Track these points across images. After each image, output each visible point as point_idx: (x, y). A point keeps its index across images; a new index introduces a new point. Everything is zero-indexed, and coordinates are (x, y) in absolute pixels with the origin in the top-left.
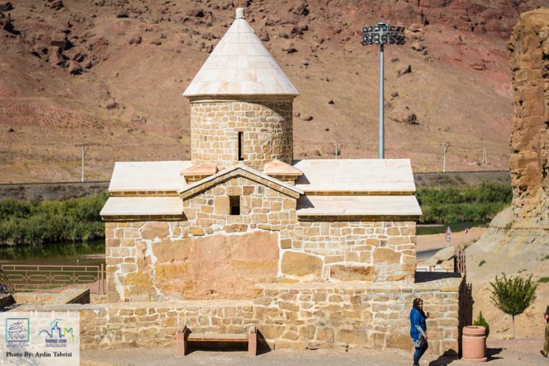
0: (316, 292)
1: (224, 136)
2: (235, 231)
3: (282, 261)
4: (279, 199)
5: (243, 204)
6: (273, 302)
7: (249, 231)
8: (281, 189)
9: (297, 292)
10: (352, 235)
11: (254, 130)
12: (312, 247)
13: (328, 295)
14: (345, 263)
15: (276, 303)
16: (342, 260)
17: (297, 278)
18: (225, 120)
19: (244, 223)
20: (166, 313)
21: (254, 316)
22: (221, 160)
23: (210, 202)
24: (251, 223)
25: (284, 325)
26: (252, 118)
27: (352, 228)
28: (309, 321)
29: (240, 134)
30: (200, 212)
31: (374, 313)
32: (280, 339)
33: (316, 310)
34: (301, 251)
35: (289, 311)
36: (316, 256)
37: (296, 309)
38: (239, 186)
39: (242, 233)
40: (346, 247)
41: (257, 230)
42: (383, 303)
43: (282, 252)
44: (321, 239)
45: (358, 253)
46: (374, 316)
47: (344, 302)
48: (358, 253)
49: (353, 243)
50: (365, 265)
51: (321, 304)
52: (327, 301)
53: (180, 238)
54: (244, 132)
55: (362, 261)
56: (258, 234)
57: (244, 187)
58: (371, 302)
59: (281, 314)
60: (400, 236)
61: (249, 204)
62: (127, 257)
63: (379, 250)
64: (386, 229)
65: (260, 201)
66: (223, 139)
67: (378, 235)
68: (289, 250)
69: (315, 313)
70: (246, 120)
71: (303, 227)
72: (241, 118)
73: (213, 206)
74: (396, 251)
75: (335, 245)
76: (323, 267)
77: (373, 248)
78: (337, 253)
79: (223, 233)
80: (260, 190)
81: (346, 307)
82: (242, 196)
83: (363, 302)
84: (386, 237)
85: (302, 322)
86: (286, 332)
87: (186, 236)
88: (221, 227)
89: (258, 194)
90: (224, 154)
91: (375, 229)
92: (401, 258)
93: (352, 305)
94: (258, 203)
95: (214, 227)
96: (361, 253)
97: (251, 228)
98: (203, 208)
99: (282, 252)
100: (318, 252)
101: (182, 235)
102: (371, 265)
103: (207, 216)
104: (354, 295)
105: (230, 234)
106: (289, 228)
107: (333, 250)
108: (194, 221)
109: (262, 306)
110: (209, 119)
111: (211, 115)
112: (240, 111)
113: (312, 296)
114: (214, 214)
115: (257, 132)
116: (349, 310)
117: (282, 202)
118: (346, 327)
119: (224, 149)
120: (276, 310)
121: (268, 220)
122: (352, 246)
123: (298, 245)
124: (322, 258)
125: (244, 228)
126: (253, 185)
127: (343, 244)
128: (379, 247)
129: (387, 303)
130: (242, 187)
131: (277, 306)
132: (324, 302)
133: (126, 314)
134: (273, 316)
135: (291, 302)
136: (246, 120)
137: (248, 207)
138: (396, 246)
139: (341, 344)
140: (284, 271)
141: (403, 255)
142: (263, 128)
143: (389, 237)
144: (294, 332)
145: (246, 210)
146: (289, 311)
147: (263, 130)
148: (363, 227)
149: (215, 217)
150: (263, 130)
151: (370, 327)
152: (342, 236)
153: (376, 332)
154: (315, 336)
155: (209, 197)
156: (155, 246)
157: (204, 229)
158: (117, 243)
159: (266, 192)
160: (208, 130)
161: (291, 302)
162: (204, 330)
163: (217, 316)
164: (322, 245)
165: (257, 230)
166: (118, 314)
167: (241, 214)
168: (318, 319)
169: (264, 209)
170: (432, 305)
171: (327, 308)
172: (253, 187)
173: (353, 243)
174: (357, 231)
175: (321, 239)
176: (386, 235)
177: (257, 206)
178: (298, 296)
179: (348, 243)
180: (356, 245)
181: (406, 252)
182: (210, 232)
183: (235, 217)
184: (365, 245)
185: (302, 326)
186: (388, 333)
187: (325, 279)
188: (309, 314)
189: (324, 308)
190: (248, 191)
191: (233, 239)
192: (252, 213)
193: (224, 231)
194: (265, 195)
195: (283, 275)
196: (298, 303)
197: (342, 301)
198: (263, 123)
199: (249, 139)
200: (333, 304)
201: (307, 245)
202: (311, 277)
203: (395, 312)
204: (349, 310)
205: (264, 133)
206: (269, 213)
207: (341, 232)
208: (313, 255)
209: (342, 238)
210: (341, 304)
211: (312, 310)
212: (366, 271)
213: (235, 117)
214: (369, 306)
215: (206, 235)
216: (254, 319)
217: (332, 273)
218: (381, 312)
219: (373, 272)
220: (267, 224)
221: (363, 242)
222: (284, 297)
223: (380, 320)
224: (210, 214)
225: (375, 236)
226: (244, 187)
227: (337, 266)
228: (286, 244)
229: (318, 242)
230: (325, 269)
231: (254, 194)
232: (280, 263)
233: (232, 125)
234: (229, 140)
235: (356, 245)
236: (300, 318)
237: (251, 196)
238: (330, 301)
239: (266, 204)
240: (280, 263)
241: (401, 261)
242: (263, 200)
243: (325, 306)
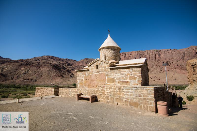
4: (106, 65)
5: (99, 67)
7: (100, 73)
8: (106, 62)
9: (105, 86)
10: (123, 72)
12: (113, 76)
13: (112, 88)
14: (121, 80)
16: (120, 79)
17: (110, 84)
21: (95, 92)
23: (93, 67)
25: (102, 95)
27: (123, 71)
28: (108, 95)
29: (105, 55)
31: (125, 94)
32: (101, 99)
33: (109, 92)
34: (111, 77)
35: (103, 91)
37: (105, 91)
39: (99, 73)
40: (121, 76)
41: (101, 72)
42: (127, 91)
43: (107, 77)
44: (115, 74)
46: (125, 95)
47: (117, 90)
48: (125, 77)
49: (123, 75)
50: (127, 80)
52: (112, 89)
53: (88, 75)
56: (102, 73)
58: (124, 90)
59: (101, 92)
63: (130, 76)
64: (132, 70)
65: (102, 65)
67: (130, 72)
69: (109, 93)
71: (111, 71)
74: (135, 76)
75: (119, 75)
77: (129, 76)
79: (95, 73)
80: (102, 63)
85: (106, 95)
86: (102, 97)
87: (89, 74)
88: (95, 72)
91: (129, 71)
92: (137, 79)
93: (118, 91)
94: (101, 66)
95: (94, 72)
99: (107, 77)
102: (128, 80)
103: (92, 70)
104: (119, 88)
105: (96, 74)
106: (108, 71)
107: (118, 77)
109: (97, 90)
116: (118, 92)
118: (117, 97)
120: (100, 91)
122: (123, 76)
123: (110, 76)
124: (116, 79)
125: (99, 72)
127: (121, 75)
131: (100, 90)
132: (111, 90)
134: (99, 92)
135: (103, 89)
138: (135, 75)
139: (116, 102)
140: (107, 82)
143: (133, 73)
144: (104, 97)
146: (103, 91)
149: (93, 70)
151: (124, 98)
153: (126, 100)
154: (109, 99)
156: (84, 76)
158: (78, 76)
161: (103, 89)
162: (86, 95)
164: (115, 75)
165: (101, 72)
168: (110, 94)
170: (144, 92)
171: (112, 91)
173: (123, 75)
174: (124, 71)
175: (115, 74)
176: (132, 72)
178: (105, 87)
181: (138, 77)
184: (126, 75)
186: (129, 101)
188: (108, 93)
190: (100, 64)
191: (97, 75)
196: (105, 89)
197: (116, 89)
200: (114, 90)
201: (112, 76)
202: (113, 84)
203: (131, 94)
204: (118, 92)
211: (108, 92)
212: (127, 82)
214: (123, 91)
216: (95, 93)
217: (118, 83)
218: (127, 94)
221: (126, 74)
222: (102, 88)
223: (127, 96)
227: (119, 81)
228: (107, 75)
229: (114, 75)
230: (116, 81)
232: (106, 80)
233: (104, 53)
235: (124, 75)
236: (105, 94)
237: (100, 65)
238: (113, 89)
239: (103, 66)
240: (106, 80)
241: (137, 80)
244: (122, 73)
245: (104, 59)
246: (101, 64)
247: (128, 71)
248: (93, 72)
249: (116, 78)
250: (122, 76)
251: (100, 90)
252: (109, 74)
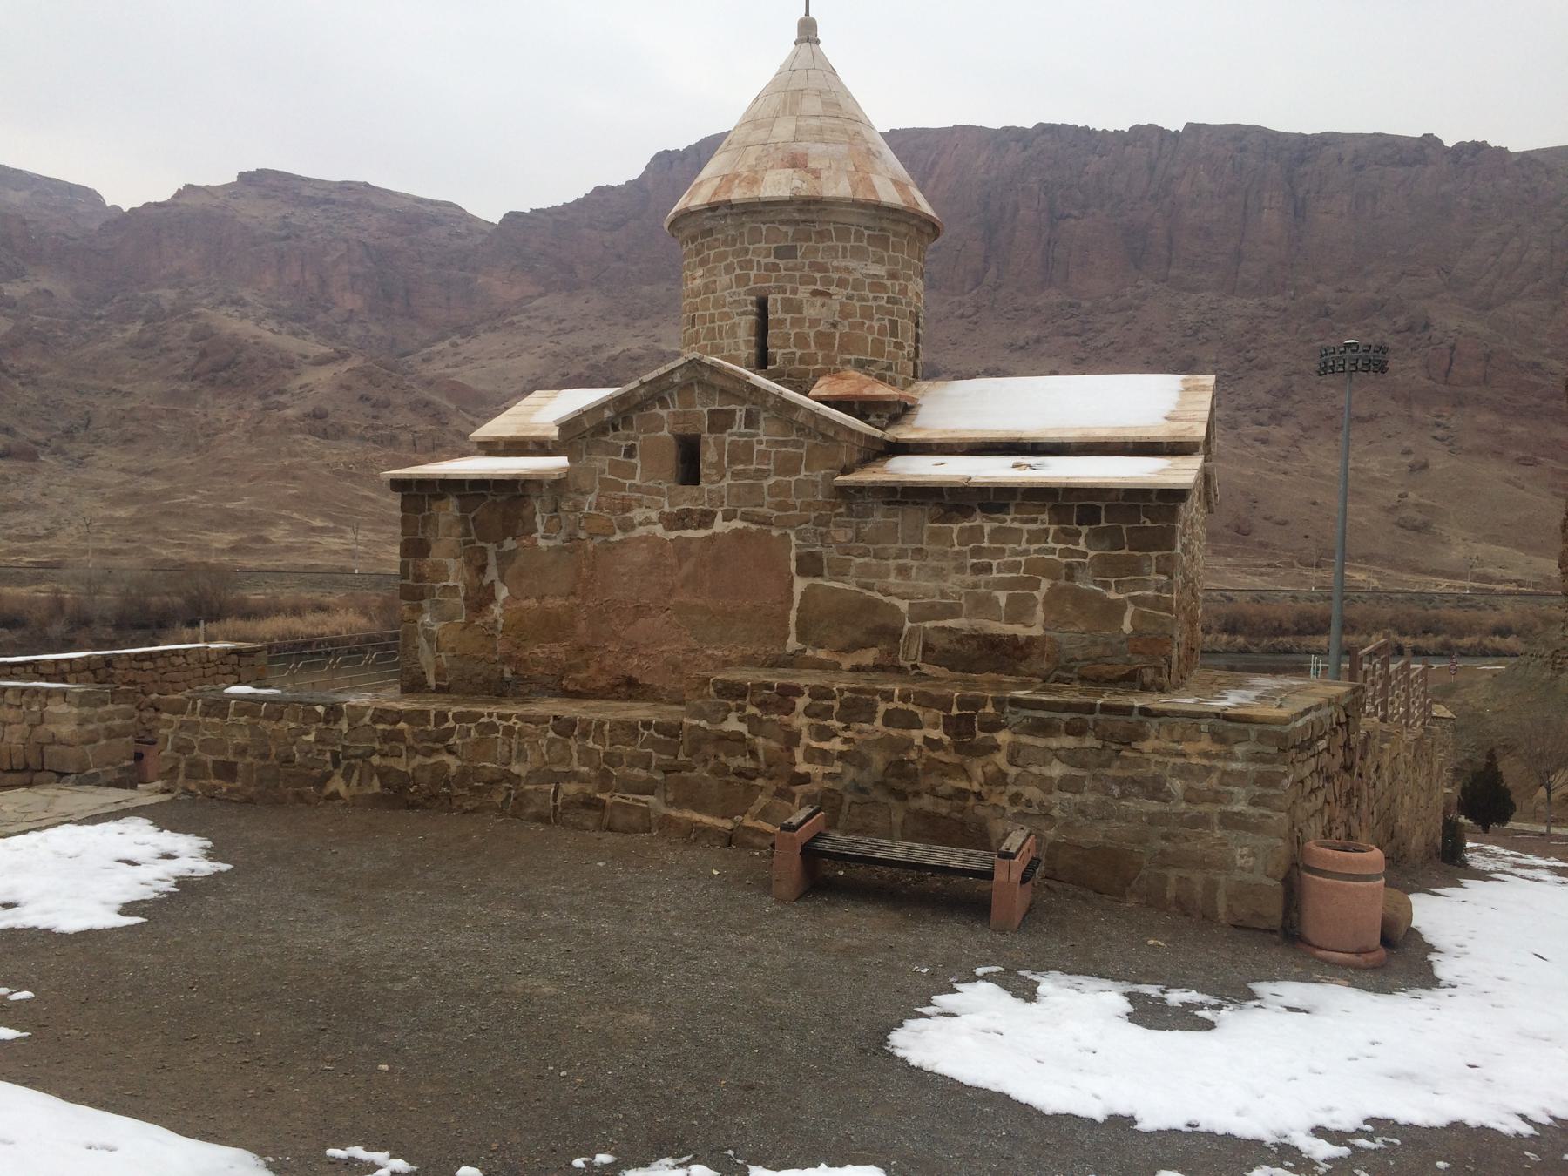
0: (847, 694)
1: (726, 309)
2: (685, 527)
3: (799, 610)
5: (709, 455)
6: (733, 717)
7: (720, 526)
9: (798, 692)
10: (986, 544)
11: (794, 291)
13: (882, 707)
15: (741, 720)
18: (729, 269)
19: (706, 507)
20: (472, 725)
24: (726, 507)
25: (760, 782)
26: (791, 262)
27: (988, 527)
29: (763, 306)
32: (748, 822)
33: (845, 748)
36: (886, 599)
38: (699, 408)
39: (701, 533)
40: (969, 578)
41: (738, 524)
43: (800, 585)
45: (1002, 597)
48: (1002, 597)
50: (1019, 630)
51: (860, 732)
52: (878, 723)
54: (770, 297)
55: (1011, 620)
57: (710, 412)
58: (1003, 737)
60: (1124, 552)
61: (721, 456)
63: (1062, 590)
68: (818, 581)
69: (842, 756)
70: (775, 267)
72: (764, 261)
73: (636, 461)
77: (1045, 584)
78: (943, 594)
79: (659, 530)
80: (751, 420)
81: (931, 743)
82: (706, 435)
83: (980, 735)
84: (1085, 555)
85: (805, 778)
87: (571, 538)
88: (654, 515)
89: (743, 430)
91: (1053, 528)
93: (947, 739)
94: (741, 453)
95: (638, 514)
96: (1010, 599)
97: (725, 519)
98: (614, 466)
99: (800, 585)
100: (892, 590)
101: (562, 535)
102: (1037, 631)
103: (622, 487)
104: (955, 711)
105: (673, 535)
108: (591, 498)
109: (703, 723)
110: (700, 272)
111: (703, 263)
112: (763, 244)
113: (836, 705)
114: (637, 481)
115: (800, 296)
117: (803, 451)
119: (726, 342)
120: (738, 738)
121: (767, 498)
122: (983, 577)
123: (840, 572)
124: (904, 605)
125: (706, 519)
126: (732, 407)
127: (960, 569)
128: (1062, 583)
129: (1054, 743)
131: (743, 728)
132: (866, 726)
133: (385, 721)
134: (731, 753)
136: (775, 267)
137: (718, 465)
140: (802, 637)
141: (1131, 609)
142: (819, 287)
143: (1092, 553)
145: (714, 471)
147: (815, 293)
148: (1016, 525)
149: (637, 489)
150: (815, 293)
152: (957, 548)
155: (628, 438)
157: (613, 518)
159: (762, 422)
163: (590, 744)
164: (903, 571)
165: (738, 524)
166: (367, 720)
167: (702, 484)
168: (852, 773)
169: (757, 470)
170: (1195, 760)
171: (878, 743)
172: (734, 411)
173: (988, 568)
177: (742, 462)
178: (802, 702)
179: (973, 566)
180: (995, 574)
182: (628, 526)
183: (689, 490)
185: (806, 787)
187: (908, 665)
188: (825, 756)
189: (866, 742)
190: (720, 421)
191: (683, 547)
192: (728, 481)
193: (660, 526)
194: (761, 432)
195: (800, 646)
196: (800, 722)
197: (918, 725)
198: (818, 275)
199: (780, 315)
205: (819, 300)
206: (771, 481)
207: (955, 536)
208: (879, 596)
209: (957, 553)
210: (917, 736)
211: (836, 745)
212: (1022, 648)
213: (751, 261)
214: (997, 748)
219: (1042, 653)
220: (765, 510)
221: (1015, 567)
224: (628, 482)
225: (1053, 551)
226: (710, 412)
231: (735, 429)
233: (742, 280)
234: (736, 319)
235: (995, 574)
236: (802, 767)
237: (727, 438)
239: (764, 455)
242: (757, 447)
243: (871, 738)
244: (977, 552)
245: (747, 351)
246: (739, 427)
247: (1046, 531)
248: (629, 509)
249: (902, 597)
250: (976, 586)
251: (743, 728)
252: (829, 553)
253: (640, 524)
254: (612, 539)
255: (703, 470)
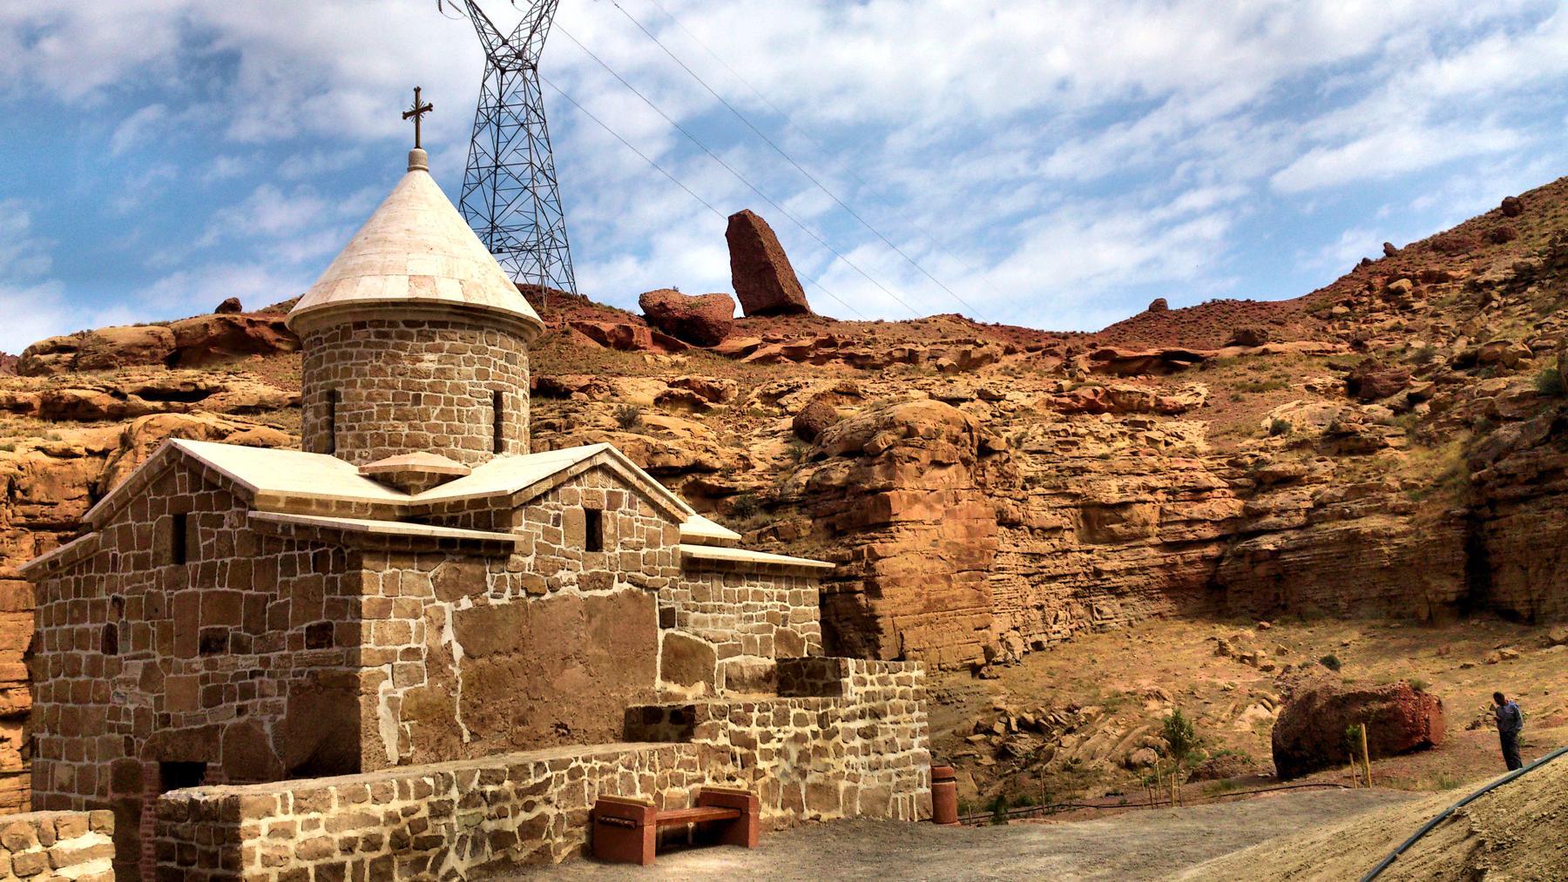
3: (663, 655)
20: (565, 772)
22: (459, 448)
30: (541, 540)
35: (745, 751)
43: (661, 635)
49: (751, 618)
53: (506, 599)
56: (630, 594)
59: (734, 759)
62: (406, 646)
66: (462, 403)
75: (727, 623)
76: (716, 666)
82: (604, 512)
88: (574, 579)
90: (466, 435)
98: (546, 531)
101: (508, 594)
103: (552, 552)
105: (587, 594)
114: (562, 546)
117: (661, 529)
120: (723, 749)
123: (683, 624)
124: (714, 647)
130: (605, 491)
131: (727, 741)
137: (614, 536)
156: (459, 617)
158: (383, 611)
160: (426, 381)
163: (647, 772)
166: (474, 785)
167: (605, 552)
172: (620, 494)
174: (758, 596)
177: (628, 535)
180: (755, 624)
182: (553, 589)
208: (703, 641)
213: (489, 360)
215: (548, 596)
231: (622, 509)
232: (659, 658)
251: (727, 741)
253: (565, 585)
254: (543, 598)
255: (606, 540)
